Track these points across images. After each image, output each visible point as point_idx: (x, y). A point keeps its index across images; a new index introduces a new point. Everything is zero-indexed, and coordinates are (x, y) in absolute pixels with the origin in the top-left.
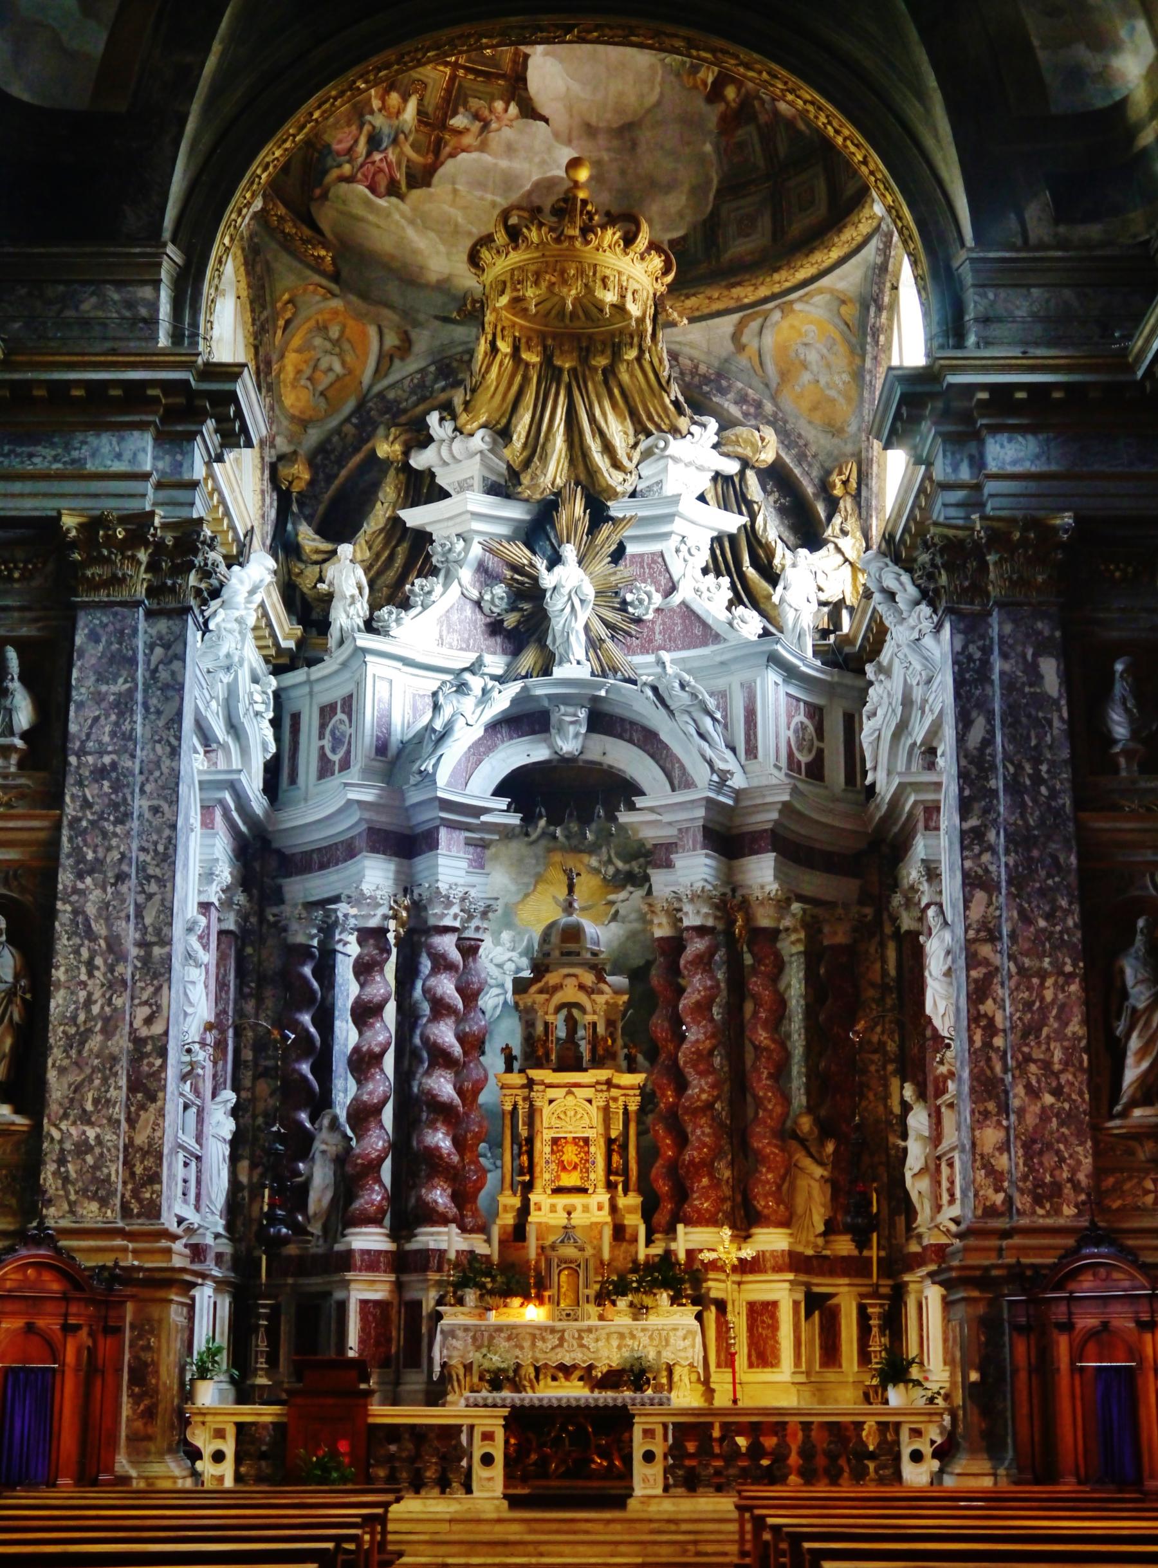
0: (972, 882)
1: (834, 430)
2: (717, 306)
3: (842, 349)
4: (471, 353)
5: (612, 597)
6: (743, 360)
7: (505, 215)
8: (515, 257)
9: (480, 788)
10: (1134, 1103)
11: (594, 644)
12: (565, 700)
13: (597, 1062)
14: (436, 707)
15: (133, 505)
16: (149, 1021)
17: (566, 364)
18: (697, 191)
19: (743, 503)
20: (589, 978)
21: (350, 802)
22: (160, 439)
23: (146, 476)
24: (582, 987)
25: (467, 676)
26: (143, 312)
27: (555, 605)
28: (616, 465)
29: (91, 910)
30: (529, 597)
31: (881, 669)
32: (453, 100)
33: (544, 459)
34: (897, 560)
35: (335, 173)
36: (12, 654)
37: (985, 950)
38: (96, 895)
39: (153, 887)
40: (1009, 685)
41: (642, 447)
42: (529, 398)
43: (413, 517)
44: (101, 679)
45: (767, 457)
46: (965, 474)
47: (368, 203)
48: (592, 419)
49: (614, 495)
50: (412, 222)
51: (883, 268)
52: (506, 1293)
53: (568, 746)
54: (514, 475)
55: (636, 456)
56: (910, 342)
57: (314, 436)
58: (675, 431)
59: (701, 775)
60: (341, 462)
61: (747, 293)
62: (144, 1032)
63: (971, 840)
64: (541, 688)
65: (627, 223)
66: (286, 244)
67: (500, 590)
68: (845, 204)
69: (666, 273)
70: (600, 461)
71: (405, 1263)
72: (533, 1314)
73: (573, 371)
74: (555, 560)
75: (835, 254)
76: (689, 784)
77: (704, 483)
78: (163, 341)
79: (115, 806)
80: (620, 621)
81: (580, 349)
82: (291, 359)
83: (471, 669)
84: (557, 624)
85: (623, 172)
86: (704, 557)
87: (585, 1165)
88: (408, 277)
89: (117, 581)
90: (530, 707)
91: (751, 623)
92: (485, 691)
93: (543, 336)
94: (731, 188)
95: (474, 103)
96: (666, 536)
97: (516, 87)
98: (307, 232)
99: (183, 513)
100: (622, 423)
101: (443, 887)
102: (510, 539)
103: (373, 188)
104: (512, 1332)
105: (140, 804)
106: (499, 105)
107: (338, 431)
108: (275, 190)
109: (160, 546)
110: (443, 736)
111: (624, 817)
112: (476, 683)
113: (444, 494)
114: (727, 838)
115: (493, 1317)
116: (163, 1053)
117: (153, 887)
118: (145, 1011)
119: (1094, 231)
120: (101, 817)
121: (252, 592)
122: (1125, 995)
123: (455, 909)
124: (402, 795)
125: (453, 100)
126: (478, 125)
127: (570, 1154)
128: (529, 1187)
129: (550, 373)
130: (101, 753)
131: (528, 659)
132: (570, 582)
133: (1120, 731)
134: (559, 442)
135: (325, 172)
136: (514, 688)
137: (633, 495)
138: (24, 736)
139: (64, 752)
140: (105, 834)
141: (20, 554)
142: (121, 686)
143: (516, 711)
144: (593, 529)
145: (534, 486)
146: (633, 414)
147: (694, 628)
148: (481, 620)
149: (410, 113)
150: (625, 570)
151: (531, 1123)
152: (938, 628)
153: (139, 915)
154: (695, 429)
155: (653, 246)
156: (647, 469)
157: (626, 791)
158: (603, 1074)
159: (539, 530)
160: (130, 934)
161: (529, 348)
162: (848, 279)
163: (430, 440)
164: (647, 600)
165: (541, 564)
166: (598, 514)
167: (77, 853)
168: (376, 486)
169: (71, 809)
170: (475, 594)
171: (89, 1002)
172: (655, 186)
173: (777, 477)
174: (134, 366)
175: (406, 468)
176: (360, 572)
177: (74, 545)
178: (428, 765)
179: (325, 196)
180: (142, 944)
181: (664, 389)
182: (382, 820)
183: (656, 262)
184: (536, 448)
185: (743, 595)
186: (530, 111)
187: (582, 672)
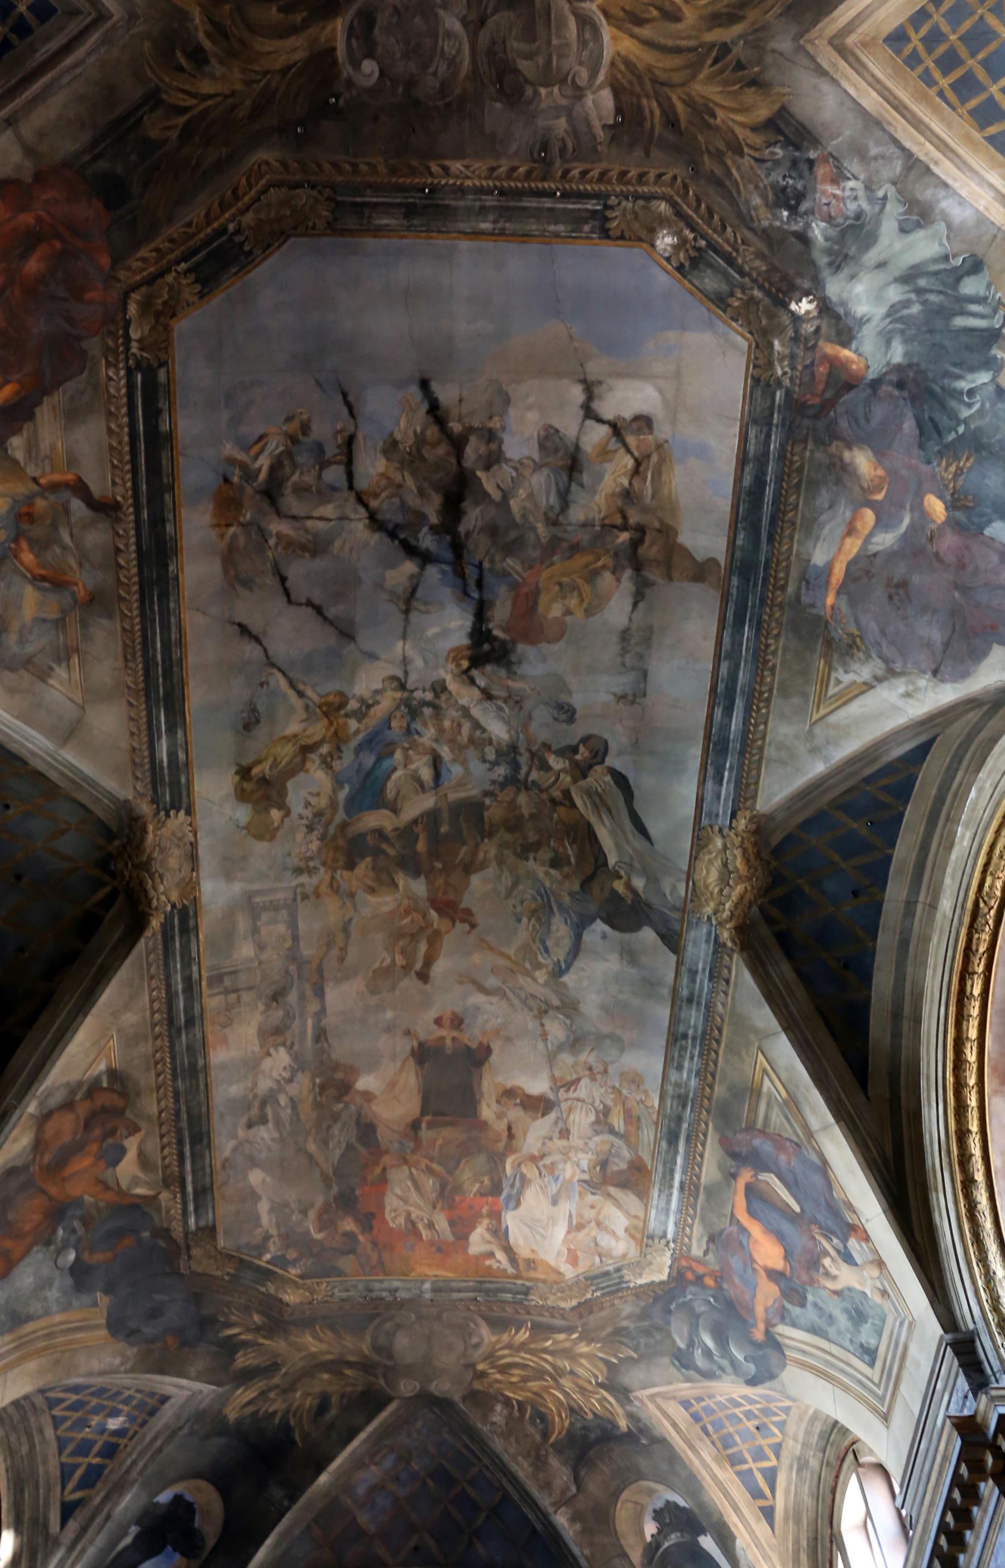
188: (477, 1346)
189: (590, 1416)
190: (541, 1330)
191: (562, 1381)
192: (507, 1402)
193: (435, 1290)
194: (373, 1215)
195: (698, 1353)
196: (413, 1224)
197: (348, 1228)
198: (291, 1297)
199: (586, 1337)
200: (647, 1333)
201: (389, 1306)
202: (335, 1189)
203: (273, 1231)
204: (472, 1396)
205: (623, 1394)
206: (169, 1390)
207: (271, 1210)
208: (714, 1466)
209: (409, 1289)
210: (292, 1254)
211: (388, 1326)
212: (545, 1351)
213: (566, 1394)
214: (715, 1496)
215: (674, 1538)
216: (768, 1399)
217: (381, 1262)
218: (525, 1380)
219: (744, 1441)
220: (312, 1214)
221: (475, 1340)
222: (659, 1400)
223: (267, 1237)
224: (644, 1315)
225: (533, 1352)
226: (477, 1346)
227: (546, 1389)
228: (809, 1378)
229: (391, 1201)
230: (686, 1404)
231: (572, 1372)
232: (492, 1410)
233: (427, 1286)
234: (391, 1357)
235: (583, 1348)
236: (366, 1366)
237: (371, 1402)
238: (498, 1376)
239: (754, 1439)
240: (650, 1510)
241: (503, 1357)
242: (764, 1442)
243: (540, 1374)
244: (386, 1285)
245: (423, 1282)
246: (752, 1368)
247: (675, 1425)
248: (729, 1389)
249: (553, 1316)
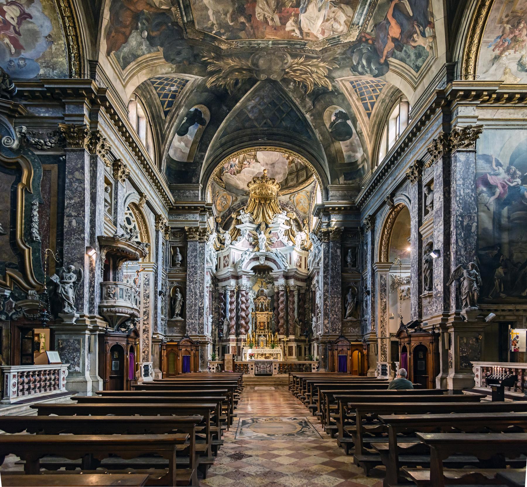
0: (325, 283)
1: (305, 213)
3: (307, 200)
4: (247, 201)
5: (269, 239)
6: (291, 202)
7: (253, 178)
8: (255, 185)
10: (348, 317)
11: (266, 247)
12: (262, 255)
17: (263, 202)
18: (284, 174)
19: (290, 225)
27: (260, 241)
28: (270, 219)
30: (256, 239)
31: (311, 251)
32: (244, 159)
33: (259, 218)
34: (315, 234)
37: (326, 294)
40: (332, 253)
42: (256, 208)
43: (238, 227)
45: (294, 217)
46: (327, 221)
47: (230, 176)
48: (266, 211)
51: (315, 187)
53: (262, 262)
54: (254, 220)
56: (319, 200)
57: (222, 214)
59: (283, 267)
60: (226, 218)
61: (292, 191)
63: (325, 277)
64: (258, 253)
65: (273, 179)
66: (217, 182)
67: (252, 238)
68: (308, 178)
70: (268, 218)
74: (260, 234)
75: (307, 185)
76: (281, 268)
77: (284, 221)
80: (271, 243)
81: (264, 200)
82: (218, 201)
84: (260, 244)
86: (283, 233)
88: (237, 188)
91: (291, 244)
94: (290, 174)
95: (248, 160)
106: (252, 160)
108: (216, 175)
111: (270, 273)
114: (287, 277)
119: (350, 182)
122: (347, 300)
125: (244, 159)
129: (260, 203)
131: (256, 249)
132: (263, 237)
133: (349, 260)
134: (261, 215)
136: (254, 254)
146: (273, 210)
147: (283, 244)
149: (237, 162)
150: (271, 235)
152: (321, 245)
155: (277, 184)
156: (275, 219)
157: (271, 269)
159: (258, 228)
162: (309, 189)
164: (274, 240)
166: (267, 226)
168: (232, 222)
172: (277, 173)
173: (296, 220)
183: (278, 186)
184: (257, 216)
185: (290, 239)
186: (257, 161)
187: (264, 251)
188: (286, 63)
189: (320, 86)
190: (308, 58)
191: (313, 75)
192: (295, 82)
193: (273, 44)
194: (251, 15)
195: (360, 66)
196: (266, 19)
197: (242, 21)
198: (224, 47)
199: (323, 61)
200: (344, 59)
201: (257, 50)
202: (236, 6)
203: (215, 22)
204: (284, 80)
205: (332, 79)
206: (188, 78)
207: (213, 13)
208: (356, 101)
209: (264, 44)
210: (222, 31)
211: (257, 56)
212: (309, 65)
213: (314, 79)
214: (354, 109)
215: (340, 121)
216: (379, 81)
217: (254, 33)
218: (301, 74)
219: (367, 94)
220: (228, 15)
221: (286, 61)
222: (343, 81)
223: (213, 25)
224: (344, 53)
225: (305, 66)
226: (286, 63)
227: (307, 77)
228: (395, 75)
229: (258, 10)
230: (352, 83)
231: (317, 72)
232: (290, 84)
233: (270, 42)
234: (258, 67)
235: (322, 64)
236: (249, 70)
237: (252, 81)
238: (292, 73)
239: (371, 93)
240: (334, 113)
241: (295, 67)
242: (373, 94)
243: (306, 73)
244: (256, 42)
245: (269, 41)
246: (377, 72)
247: (347, 89)
248: (368, 78)
249: (313, 53)
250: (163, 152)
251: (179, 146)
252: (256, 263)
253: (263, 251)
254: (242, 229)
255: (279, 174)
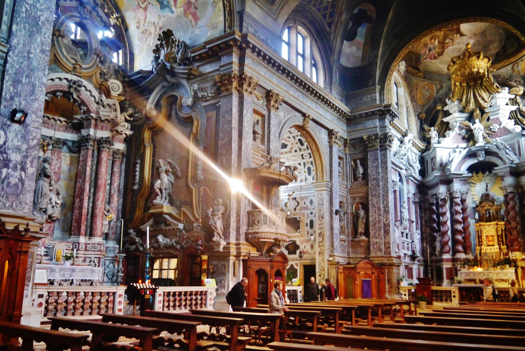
2: (507, 64)
5: (487, 128)
6: (515, 73)
7: (452, 60)
8: (455, 67)
9: (463, 170)
11: (484, 138)
12: (479, 150)
13: (494, 220)
14: (450, 156)
15: (375, 132)
16: (386, 221)
18: (500, 41)
20: (491, 204)
21: (435, 176)
22: (380, 120)
23: (377, 127)
24: (490, 206)
25: (456, 149)
26: (374, 98)
27: (475, 132)
29: (375, 203)
32: (445, 37)
33: (469, 103)
35: (422, 58)
36: (358, 162)
38: (375, 200)
39: (385, 198)
41: (491, 97)
42: (465, 92)
44: (373, 163)
49: (485, 108)
50: (440, 63)
52: (473, 266)
53: (481, 159)
55: (490, 99)
58: (498, 92)
61: (513, 60)
62: (386, 223)
64: (473, 149)
66: (413, 74)
69: (489, 61)
70: (481, 102)
71: (454, 260)
72: (479, 269)
73: (474, 85)
78: (378, 102)
79: (377, 184)
80: (490, 133)
83: (457, 148)
84: (476, 136)
85: (484, 41)
87: (493, 241)
88: (439, 74)
89: (374, 146)
90: (472, 152)
92: (460, 151)
93: (466, 80)
95: (450, 37)
96: (499, 113)
97: (458, 31)
98: (417, 71)
99: (384, 132)
100: (485, 92)
101: (455, 189)
102: (465, 120)
103: (431, 59)
104: (474, 273)
105: (381, 184)
106: (455, 35)
107: (430, 106)
109: (381, 138)
110: (451, 161)
112: (458, 150)
113: (451, 114)
115: (471, 270)
116: (389, 226)
117: (385, 198)
118: (385, 219)
120: (375, 187)
121: (409, 141)
123: (459, 193)
124: (445, 173)
125: (445, 37)
126: (451, 41)
127: (490, 238)
128: (482, 245)
129: (469, 87)
130: (374, 176)
131: (471, 143)
134: (472, 100)
135: (420, 59)
136: (467, 149)
137: (491, 106)
138: (362, 174)
139: (368, 176)
140: (376, 190)
141: (358, 144)
142: (376, 164)
143: (469, 154)
144: (482, 115)
145: (468, 109)
146: (488, 91)
148: (460, 137)
149: (437, 42)
151: (481, 233)
153: (383, 202)
154: (503, 91)
156: (492, 101)
158: (496, 222)
160: (382, 206)
161: (463, 83)
163: (447, 104)
165: (471, 124)
166: (483, 112)
167: (372, 193)
169: (370, 186)
170: (459, 132)
171: (376, 218)
172: (491, 42)
174: (371, 108)
175: (443, 110)
176: (436, 132)
177: (366, 141)
178: (449, 167)
179: (421, 63)
180: (384, 208)
181: (493, 84)
182: (442, 178)
184: (468, 102)
186: (462, 35)
187: (482, 144)
250: (333, 63)
251: (350, 53)
252: (472, 161)
253: (481, 143)
254: (451, 122)
255: (494, 42)
